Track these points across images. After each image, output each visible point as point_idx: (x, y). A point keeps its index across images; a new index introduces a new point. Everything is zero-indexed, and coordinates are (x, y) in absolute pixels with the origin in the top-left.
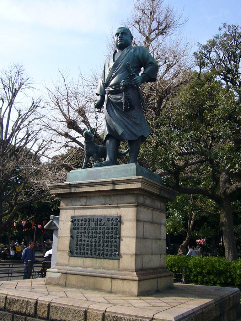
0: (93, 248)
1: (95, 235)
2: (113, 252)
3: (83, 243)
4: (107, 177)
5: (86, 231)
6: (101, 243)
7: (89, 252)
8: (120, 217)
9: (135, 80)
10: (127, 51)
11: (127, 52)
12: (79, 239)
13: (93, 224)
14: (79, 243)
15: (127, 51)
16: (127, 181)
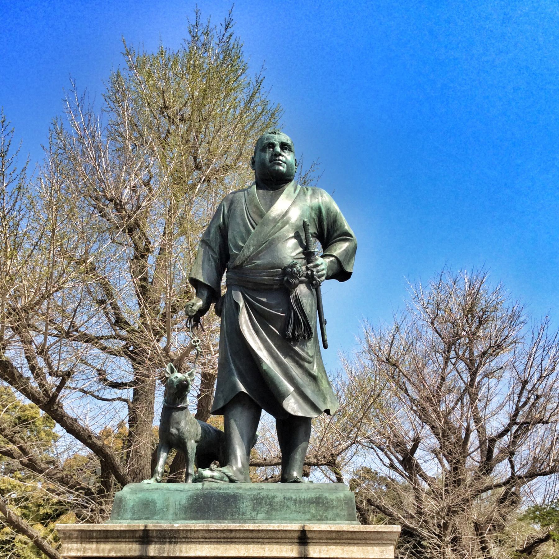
11: (297, 191)
16: (349, 535)
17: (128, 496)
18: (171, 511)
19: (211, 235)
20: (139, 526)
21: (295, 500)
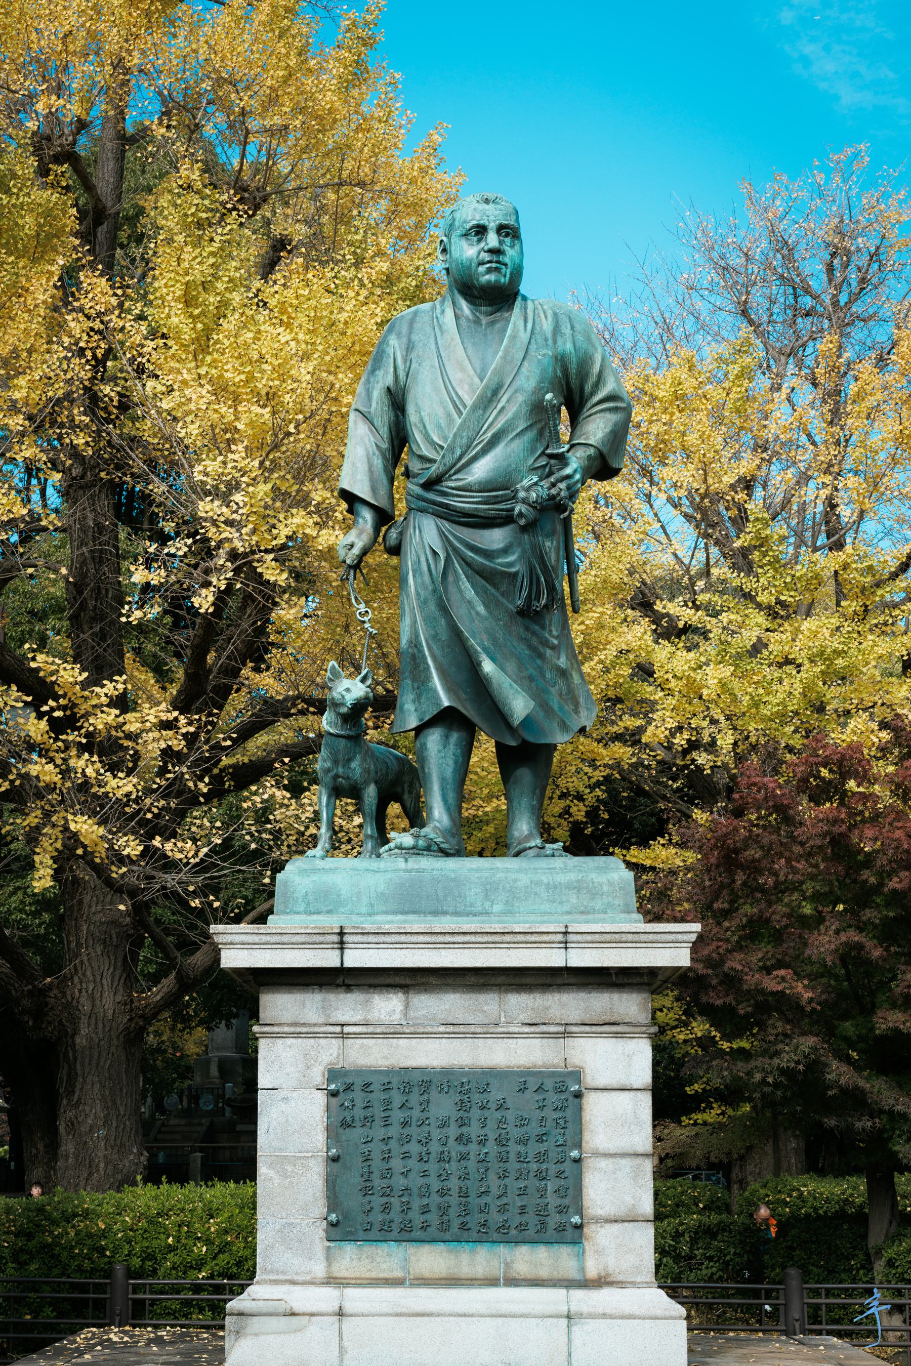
0: (454, 1200)
1: (462, 1148)
2: (556, 1219)
3: (400, 1182)
4: (497, 908)
5: (413, 1130)
6: (493, 1181)
7: (433, 1218)
8: (577, 1075)
9: (568, 477)
10: (525, 326)
11: (529, 325)
12: (377, 1164)
13: (443, 1106)
14: (377, 1182)
15: (525, 326)
17: (297, 879)
18: (365, 900)
19: (374, 404)
20: (332, 928)
21: (548, 886)
